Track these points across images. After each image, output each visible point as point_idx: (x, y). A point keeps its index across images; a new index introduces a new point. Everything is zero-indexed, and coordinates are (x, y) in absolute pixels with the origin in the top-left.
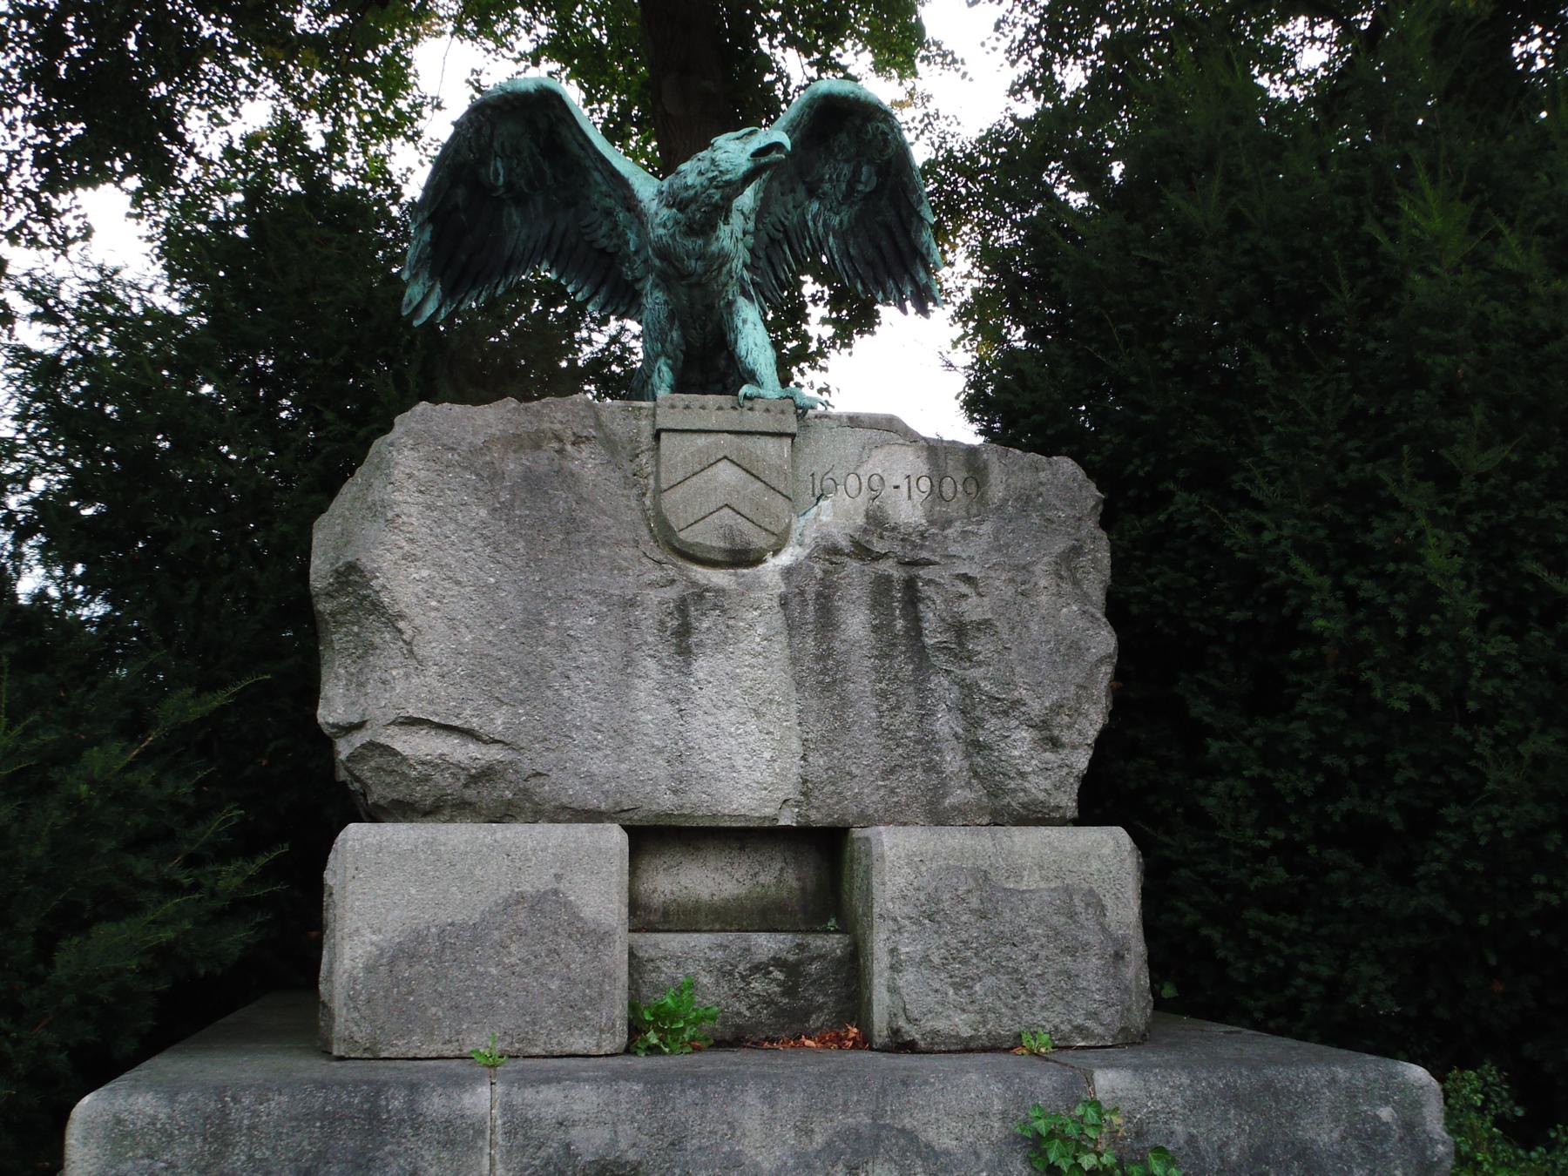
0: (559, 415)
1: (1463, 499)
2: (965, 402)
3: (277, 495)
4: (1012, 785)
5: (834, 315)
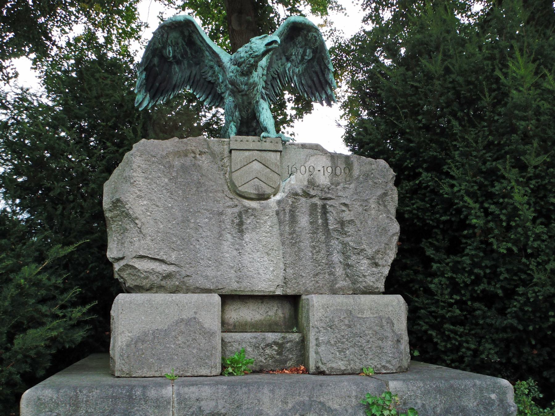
0: (194, 144)
1: (529, 175)
2: (345, 139)
3: (90, 174)
4: (361, 280)
5: (296, 106)
